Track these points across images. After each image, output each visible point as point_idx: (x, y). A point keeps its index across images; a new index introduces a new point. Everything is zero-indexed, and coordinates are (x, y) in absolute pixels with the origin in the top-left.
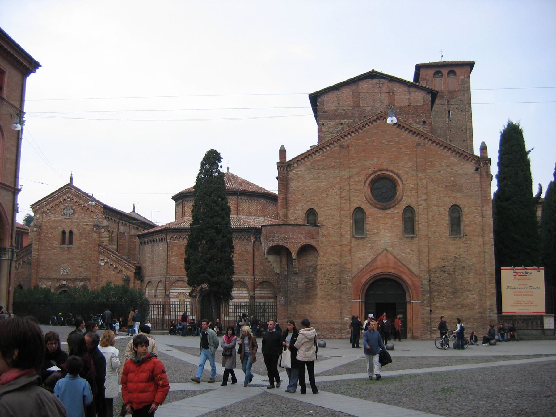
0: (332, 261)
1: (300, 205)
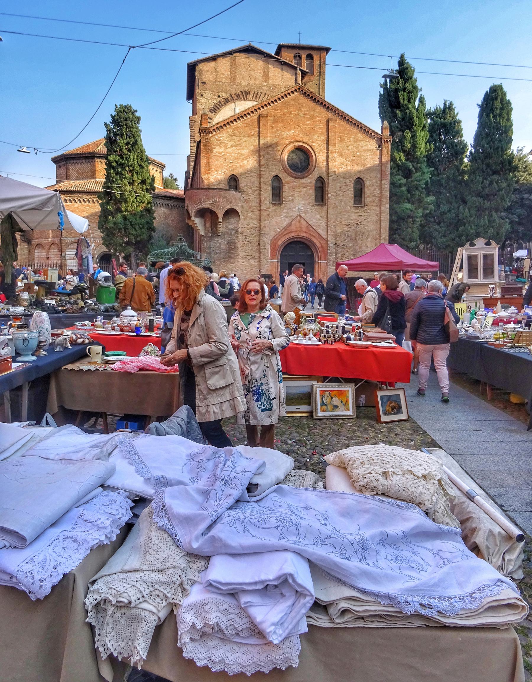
0: (252, 225)
1: (223, 171)
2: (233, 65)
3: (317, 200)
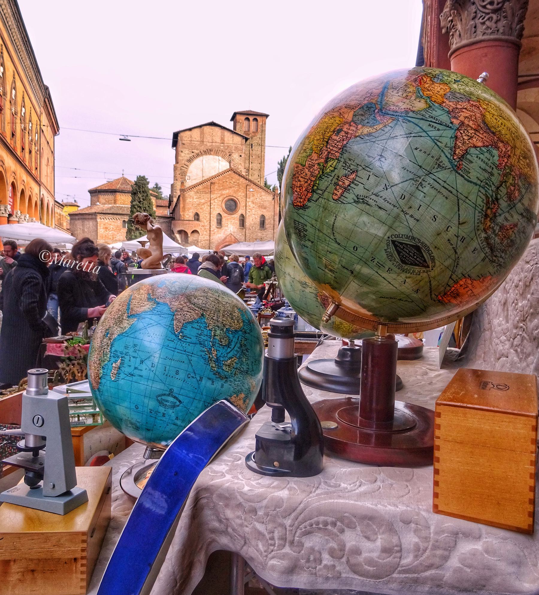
0: (206, 238)
2: (202, 133)
3: (240, 226)
